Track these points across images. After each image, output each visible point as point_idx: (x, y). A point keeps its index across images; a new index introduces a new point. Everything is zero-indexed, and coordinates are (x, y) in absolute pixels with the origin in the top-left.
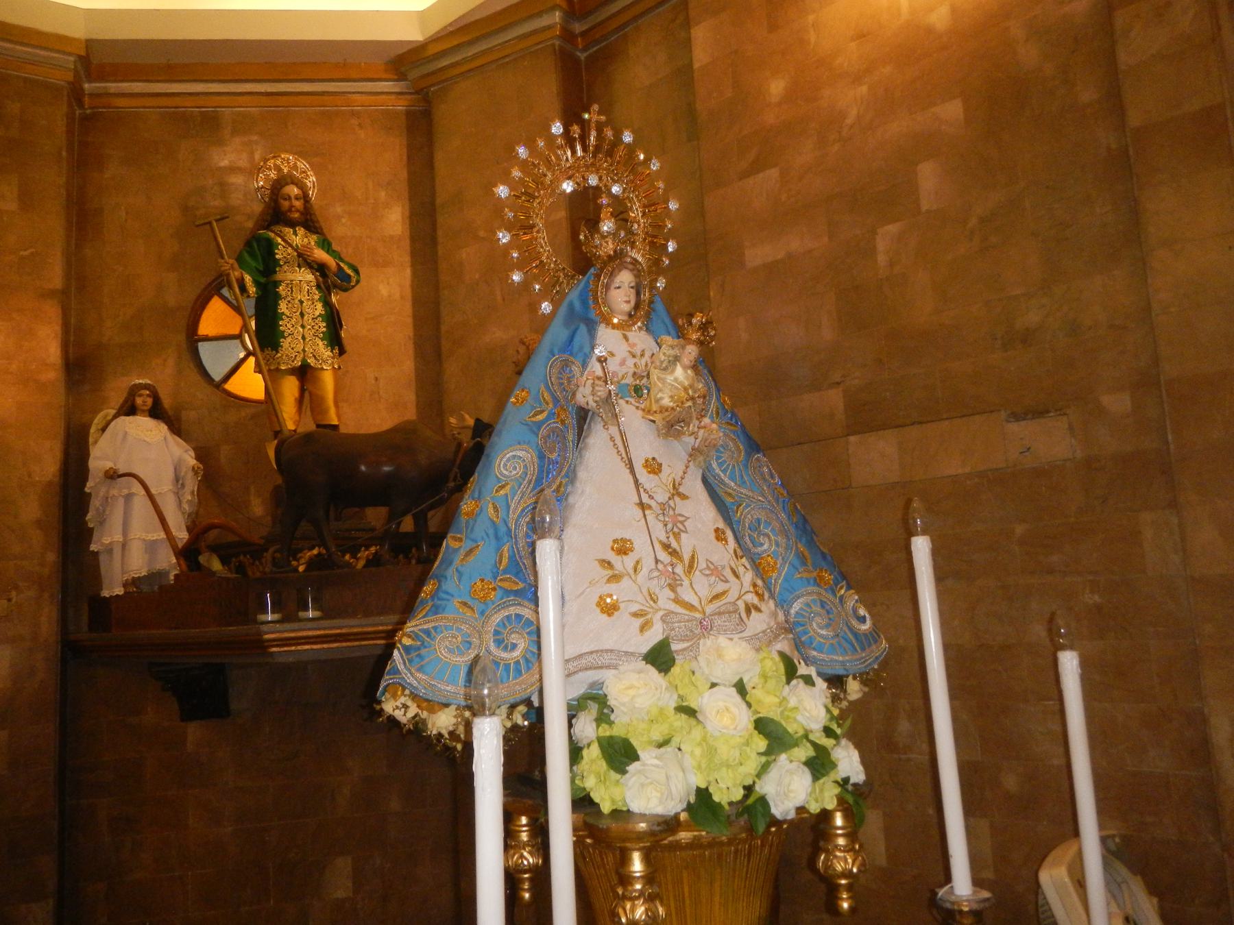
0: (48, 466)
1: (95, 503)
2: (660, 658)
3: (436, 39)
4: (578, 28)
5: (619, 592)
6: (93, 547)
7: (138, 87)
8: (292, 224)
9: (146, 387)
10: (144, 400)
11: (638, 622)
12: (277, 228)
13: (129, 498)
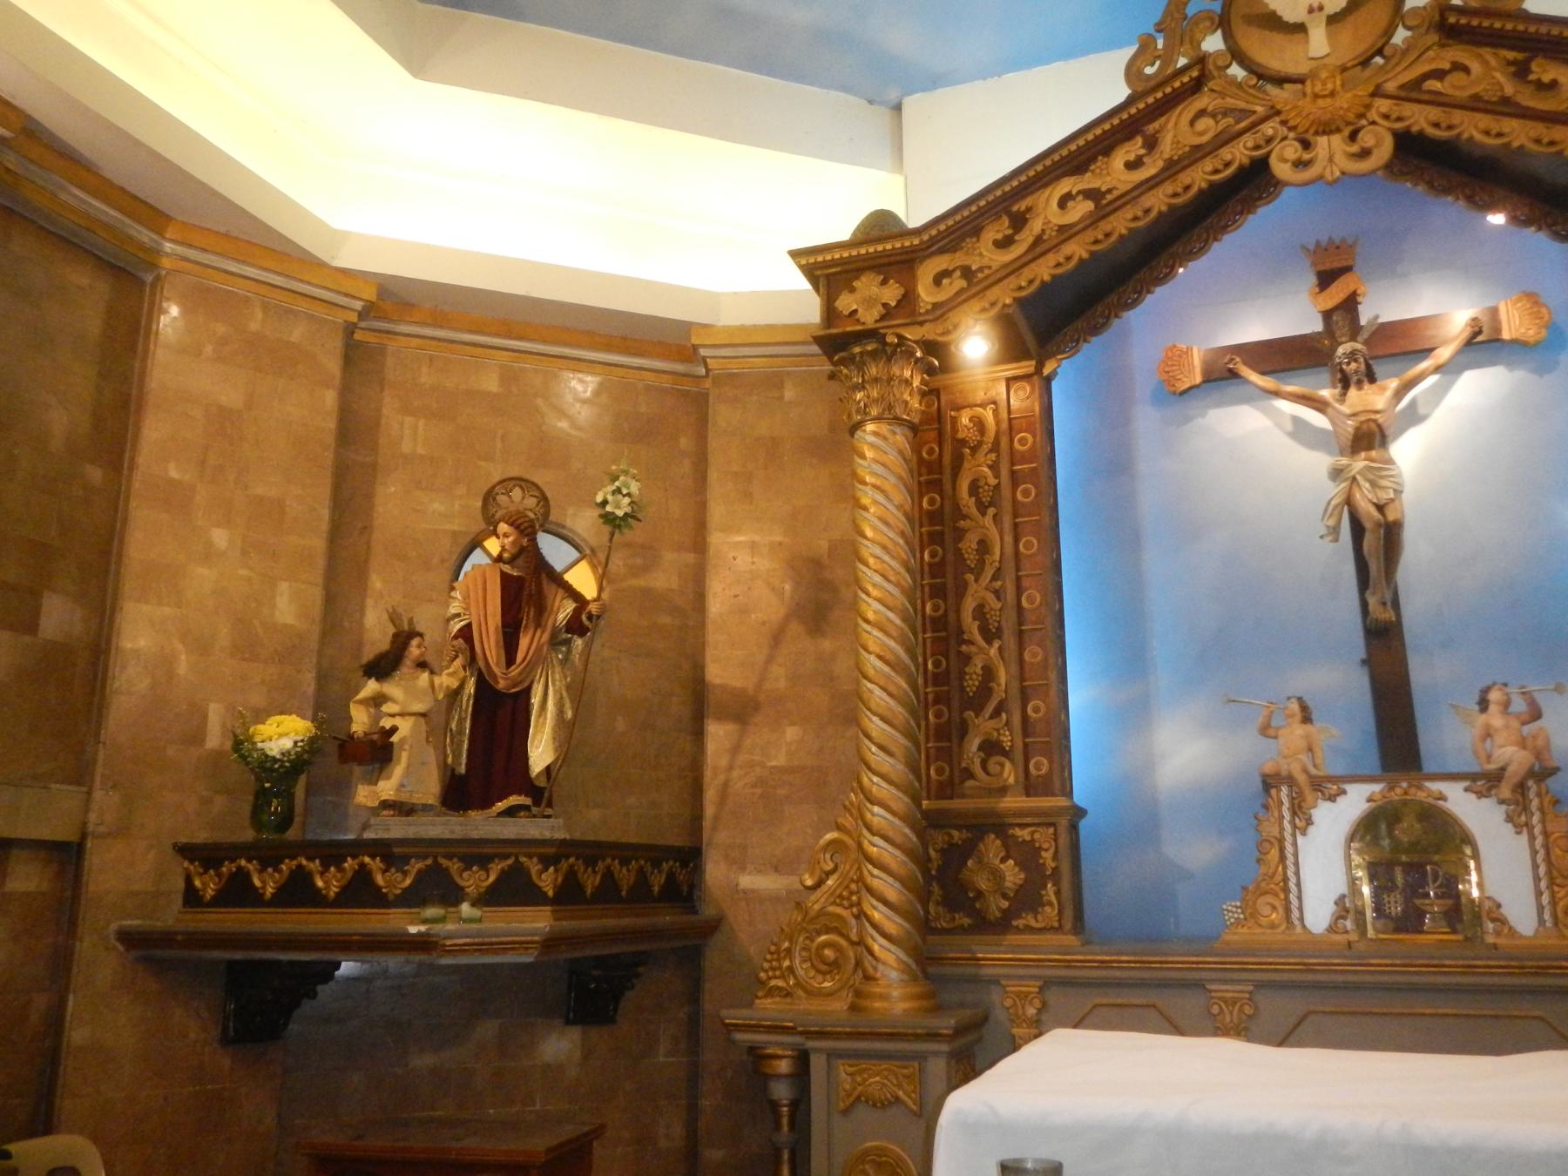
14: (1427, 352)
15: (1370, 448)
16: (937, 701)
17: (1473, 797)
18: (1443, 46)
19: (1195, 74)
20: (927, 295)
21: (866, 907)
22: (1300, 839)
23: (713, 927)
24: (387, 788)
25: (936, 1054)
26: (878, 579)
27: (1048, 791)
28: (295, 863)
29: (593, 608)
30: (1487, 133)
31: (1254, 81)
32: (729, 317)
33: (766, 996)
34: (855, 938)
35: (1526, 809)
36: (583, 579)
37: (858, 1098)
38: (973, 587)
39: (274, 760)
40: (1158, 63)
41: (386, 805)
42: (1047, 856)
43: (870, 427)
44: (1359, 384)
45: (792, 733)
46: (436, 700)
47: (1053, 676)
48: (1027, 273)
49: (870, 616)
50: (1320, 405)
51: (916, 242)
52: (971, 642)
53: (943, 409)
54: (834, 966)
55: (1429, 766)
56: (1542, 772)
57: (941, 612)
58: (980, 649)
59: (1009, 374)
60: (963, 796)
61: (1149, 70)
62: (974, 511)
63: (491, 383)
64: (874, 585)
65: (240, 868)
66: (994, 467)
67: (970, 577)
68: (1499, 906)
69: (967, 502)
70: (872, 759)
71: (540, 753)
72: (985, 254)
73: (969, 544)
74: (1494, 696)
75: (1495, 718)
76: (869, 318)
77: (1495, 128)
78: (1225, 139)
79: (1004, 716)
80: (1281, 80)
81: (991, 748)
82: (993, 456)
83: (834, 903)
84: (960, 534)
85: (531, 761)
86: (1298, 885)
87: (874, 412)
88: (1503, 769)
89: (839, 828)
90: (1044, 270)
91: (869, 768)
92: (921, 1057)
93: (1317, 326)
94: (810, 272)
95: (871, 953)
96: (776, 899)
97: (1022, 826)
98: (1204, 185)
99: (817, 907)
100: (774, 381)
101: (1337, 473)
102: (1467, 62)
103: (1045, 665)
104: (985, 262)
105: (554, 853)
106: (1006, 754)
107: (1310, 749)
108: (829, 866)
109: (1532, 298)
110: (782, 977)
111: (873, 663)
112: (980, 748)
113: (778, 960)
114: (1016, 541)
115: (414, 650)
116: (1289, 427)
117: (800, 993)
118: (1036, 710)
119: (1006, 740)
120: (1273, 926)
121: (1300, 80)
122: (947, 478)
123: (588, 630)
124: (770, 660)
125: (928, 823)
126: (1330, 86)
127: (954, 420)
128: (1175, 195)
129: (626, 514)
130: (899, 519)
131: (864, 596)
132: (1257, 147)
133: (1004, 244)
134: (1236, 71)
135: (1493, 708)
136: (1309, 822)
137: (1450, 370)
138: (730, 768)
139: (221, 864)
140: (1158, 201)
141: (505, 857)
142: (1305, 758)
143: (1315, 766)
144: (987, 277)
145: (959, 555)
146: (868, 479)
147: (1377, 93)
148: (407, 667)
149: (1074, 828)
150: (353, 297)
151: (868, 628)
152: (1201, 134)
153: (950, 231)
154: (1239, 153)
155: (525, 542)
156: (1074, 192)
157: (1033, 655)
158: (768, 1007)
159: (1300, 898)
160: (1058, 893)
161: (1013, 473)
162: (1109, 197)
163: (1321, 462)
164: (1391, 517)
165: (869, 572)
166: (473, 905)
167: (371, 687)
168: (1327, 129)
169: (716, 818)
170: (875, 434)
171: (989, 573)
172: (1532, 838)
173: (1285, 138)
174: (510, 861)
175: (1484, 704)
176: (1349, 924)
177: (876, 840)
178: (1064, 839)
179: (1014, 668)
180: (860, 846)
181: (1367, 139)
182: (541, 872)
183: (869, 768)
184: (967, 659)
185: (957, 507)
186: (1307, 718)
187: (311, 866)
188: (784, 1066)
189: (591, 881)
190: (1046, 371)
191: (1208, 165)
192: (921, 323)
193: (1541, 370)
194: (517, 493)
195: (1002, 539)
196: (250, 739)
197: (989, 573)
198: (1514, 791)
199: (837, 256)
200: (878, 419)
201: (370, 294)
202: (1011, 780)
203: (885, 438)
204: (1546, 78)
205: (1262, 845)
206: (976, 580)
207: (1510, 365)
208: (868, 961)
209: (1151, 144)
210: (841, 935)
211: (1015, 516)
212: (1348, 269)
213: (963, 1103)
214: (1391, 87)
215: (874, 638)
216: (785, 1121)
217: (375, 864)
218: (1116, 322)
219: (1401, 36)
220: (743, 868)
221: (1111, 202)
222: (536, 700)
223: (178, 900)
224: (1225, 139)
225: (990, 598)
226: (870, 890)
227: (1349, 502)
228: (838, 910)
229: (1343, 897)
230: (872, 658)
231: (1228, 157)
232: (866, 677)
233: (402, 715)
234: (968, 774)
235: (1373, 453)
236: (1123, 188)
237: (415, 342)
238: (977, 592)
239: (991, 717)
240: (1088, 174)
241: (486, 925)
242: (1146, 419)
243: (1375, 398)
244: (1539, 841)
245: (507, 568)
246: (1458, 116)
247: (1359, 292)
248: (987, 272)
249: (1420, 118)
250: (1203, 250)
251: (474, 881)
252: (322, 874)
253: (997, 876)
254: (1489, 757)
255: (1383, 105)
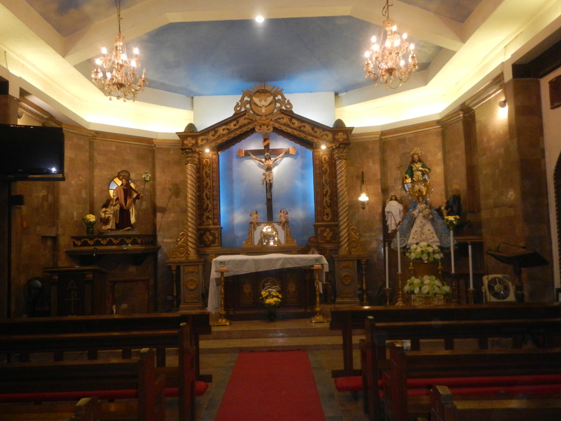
0: (380, 210)
1: (386, 217)
2: (417, 244)
3: (443, 118)
4: (467, 115)
5: (415, 237)
6: (387, 224)
7: (391, 136)
8: (416, 163)
9: (394, 195)
10: (394, 198)
11: (415, 240)
12: (414, 163)
13: (391, 216)
14: (278, 154)
15: (269, 170)
16: (199, 210)
17: (278, 225)
18: (281, 114)
19: (245, 113)
20: (199, 142)
21: (189, 244)
22: (254, 232)
23: (160, 247)
24: (109, 227)
25: (200, 264)
26: (191, 191)
27: (217, 225)
28: (97, 239)
29: (142, 195)
30: (285, 129)
31: (254, 114)
32: (160, 137)
33: (171, 258)
34: (186, 248)
35: (284, 227)
36: (132, 185)
37: (188, 272)
38: (205, 191)
39: (92, 222)
40: (239, 107)
41: (109, 229)
42: (217, 235)
43: (189, 164)
44: (268, 160)
45: (173, 215)
46: (114, 212)
47: (218, 206)
48: (217, 141)
49: (189, 197)
50: (262, 162)
51: (199, 134)
52: (205, 200)
53: (200, 158)
54: (183, 253)
55: (274, 221)
56: (287, 222)
57: (199, 195)
58: (207, 201)
59: (212, 153)
60: (203, 226)
61: (238, 109)
62: (206, 177)
63: (114, 149)
64: (190, 192)
65: (85, 240)
66: (209, 170)
67: (205, 189)
68: (280, 240)
69: (205, 176)
70: (189, 220)
71: (133, 220)
72: (210, 136)
73: (205, 183)
74: (282, 211)
75: (282, 214)
76: (190, 145)
77: (286, 129)
78: (249, 123)
79: (210, 213)
80: (258, 115)
81: (208, 218)
82: (209, 168)
83: (183, 243)
84: (203, 181)
85: (132, 221)
86: (254, 238)
87: (190, 162)
88: (282, 221)
89: (184, 231)
90: (220, 141)
91: (189, 222)
92: (198, 265)
93: (263, 148)
94: (179, 136)
95: (189, 250)
96: (170, 243)
97: (213, 230)
98: (245, 131)
99: (180, 244)
100: (168, 150)
101: (264, 174)
102: (283, 117)
103: (217, 204)
104: (210, 138)
105: (139, 236)
106: (211, 219)
107: (257, 218)
108: (182, 237)
109: (294, 147)
110: (174, 255)
111: (189, 205)
112: (206, 218)
113: (174, 253)
114: (213, 183)
115: (111, 203)
116: (258, 164)
117: (177, 257)
118: (215, 212)
119: (210, 216)
120: (250, 244)
121: (261, 116)
122: (201, 171)
123: (140, 198)
124: (169, 202)
125: (198, 230)
126: (264, 119)
127: (202, 161)
128: (241, 132)
129: (149, 180)
130: (194, 181)
131: (188, 193)
132: (254, 126)
133: (213, 135)
134: (251, 112)
135: (282, 212)
136: (256, 229)
137: (283, 157)
138: (162, 221)
139: (81, 239)
140: (238, 132)
141: (132, 237)
142: (256, 220)
143: (257, 221)
144: (210, 141)
145: (202, 184)
146: (189, 173)
147: (271, 120)
148: (109, 206)
149: (221, 230)
150: (91, 134)
151: (189, 199)
152: (245, 122)
153: (205, 133)
154: (251, 126)
155: (127, 182)
156: (225, 128)
157: (215, 202)
158: (172, 260)
159: (254, 240)
160: (218, 241)
161: (213, 171)
162: (231, 130)
163: (263, 171)
164: (271, 182)
165: (189, 190)
166: (131, 245)
167: (104, 209)
168: (264, 125)
169: (159, 230)
170: (190, 165)
171: (208, 188)
172: (285, 231)
173: (257, 125)
174: (133, 238)
175: (281, 212)
176: (260, 244)
177: (190, 233)
178: (219, 232)
179: (212, 205)
180: (188, 235)
181: (269, 127)
182: (138, 240)
183: (189, 222)
184: (204, 203)
185: (203, 176)
186: (257, 213)
187: (100, 239)
188: (174, 269)
189: (144, 241)
190: (218, 154)
191: (246, 127)
192: (199, 148)
193: (295, 159)
194: (124, 173)
195: (210, 183)
196: (86, 219)
197: (208, 188)
198: (283, 224)
199: (184, 134)
200: (190, 163)
201: (94, 134)
202: (211, 223)
203: (192, 166)
204: (294, 122)
205: (249, 233)
206: (206, 189)
207: (291, 157)
208: (189, 252)
209: (238, 122)
210: (185, 248)
211: (213, 178)
212: (268, 139)
213: (214, 259)
214: (273, 119)
215: (189, 200)
216: (175, 278)
217: (113, 239)
218: (231, 147)
219: (275, 111)
220: (164, 238)
221: (230, 132)
222: (131, 211)
223: (72, 246)
224: (249, 123)
225: (209, 194)
226: (189, 241)
227: (265, 179)
228: (184, 244)
229: (260, 240)
230: (190, 204)
231: (249, 127)
232: (188, 207)
233: (110, 214)
234: (204, 222)
235: (269, 171)
236: (233, 129)
237: (99, 141)
238: (206, 191)
239: (208, 213)
240: (227, 126)
241: (133, 248)
242: (235, 161)
243: (270, 162)
244: (286, 231)
245: (124, 187)
246: (282, 126)
247: (270, 143)
248: (210, 140)
249: (277, 125)
250: (245, 138)
251: (128, 241)
252: (102, 241)
253: (208, 238)
254: (280, 220)
255: (272, 122)
